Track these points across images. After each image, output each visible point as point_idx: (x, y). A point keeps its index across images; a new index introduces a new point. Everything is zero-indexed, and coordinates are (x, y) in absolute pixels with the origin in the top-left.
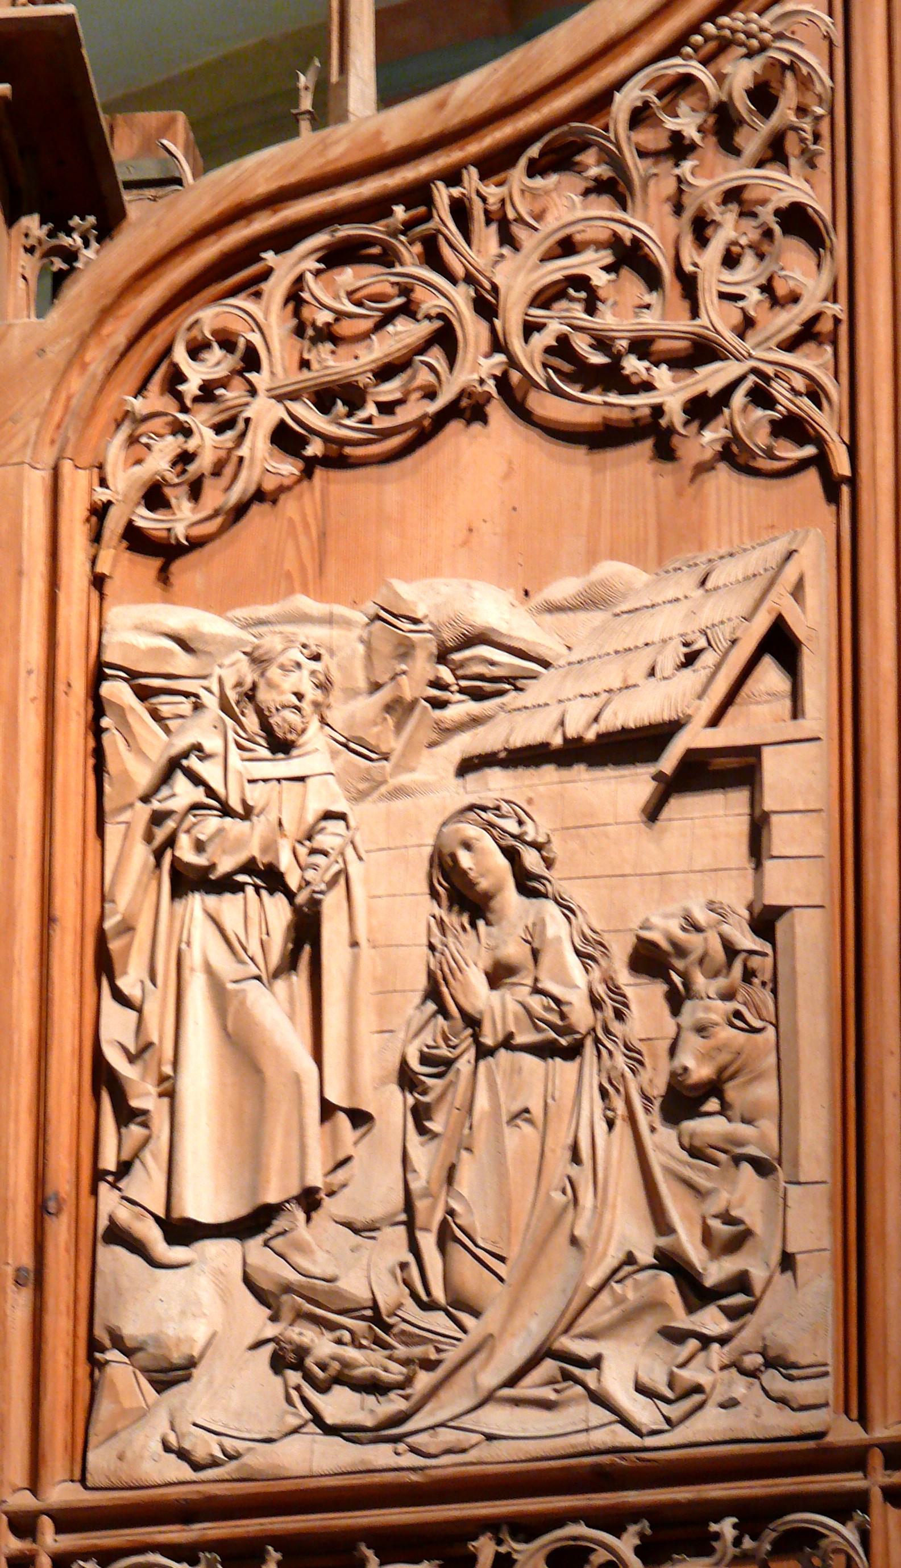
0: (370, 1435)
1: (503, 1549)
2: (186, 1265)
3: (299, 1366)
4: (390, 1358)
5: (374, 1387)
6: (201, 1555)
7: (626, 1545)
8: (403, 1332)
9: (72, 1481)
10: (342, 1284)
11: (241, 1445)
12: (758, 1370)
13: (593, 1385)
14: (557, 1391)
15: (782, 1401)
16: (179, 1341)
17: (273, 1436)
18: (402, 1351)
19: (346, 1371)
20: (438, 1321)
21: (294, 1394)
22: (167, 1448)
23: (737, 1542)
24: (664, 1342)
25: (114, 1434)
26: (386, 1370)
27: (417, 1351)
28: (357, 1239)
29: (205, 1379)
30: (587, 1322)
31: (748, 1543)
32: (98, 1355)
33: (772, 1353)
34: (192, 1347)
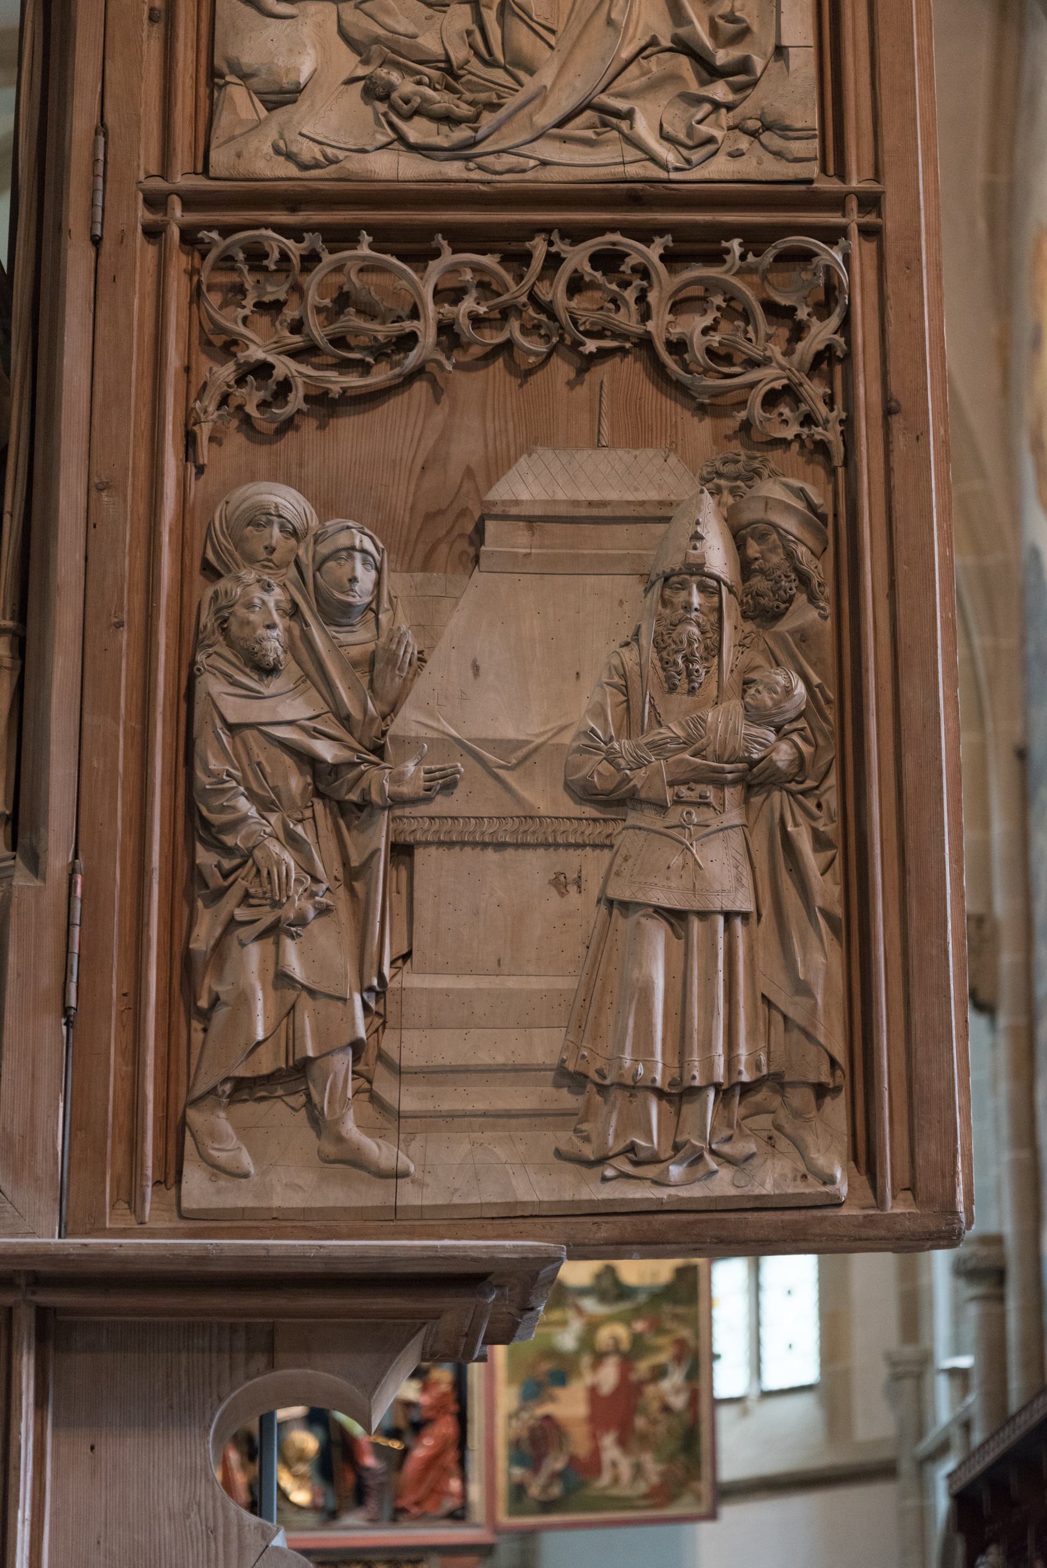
0: (446, 154)
1: (553, 249)
2: (292, 17)
3: (385, 98)
4: (459, 99)
5: (448, 119)
6: (305, 234)
7: (654, 252)
8: (469, 81)
9: (196, 173)
10: (420, 40)
11: (341, 154)
12: (757, 131)
13: (626, 130)
14: (598, 134)
15: (778, 154)
16: (288, 71)
17: (368, 148)
18: (468, 96)
19: (425, 105)
20: (498, 75)
21: (383, 119)
22: (277, 151)
23: (743, 257)
24: (683, 105)
25: (232, 138)
26: (458, 107)
27: (483, 96)
28: (429, 11)
29: (308, 103)
30: (619, 85)
31: (751, 258)
32: (216, 80)
33: (769, 119)
34: (299, 76)
